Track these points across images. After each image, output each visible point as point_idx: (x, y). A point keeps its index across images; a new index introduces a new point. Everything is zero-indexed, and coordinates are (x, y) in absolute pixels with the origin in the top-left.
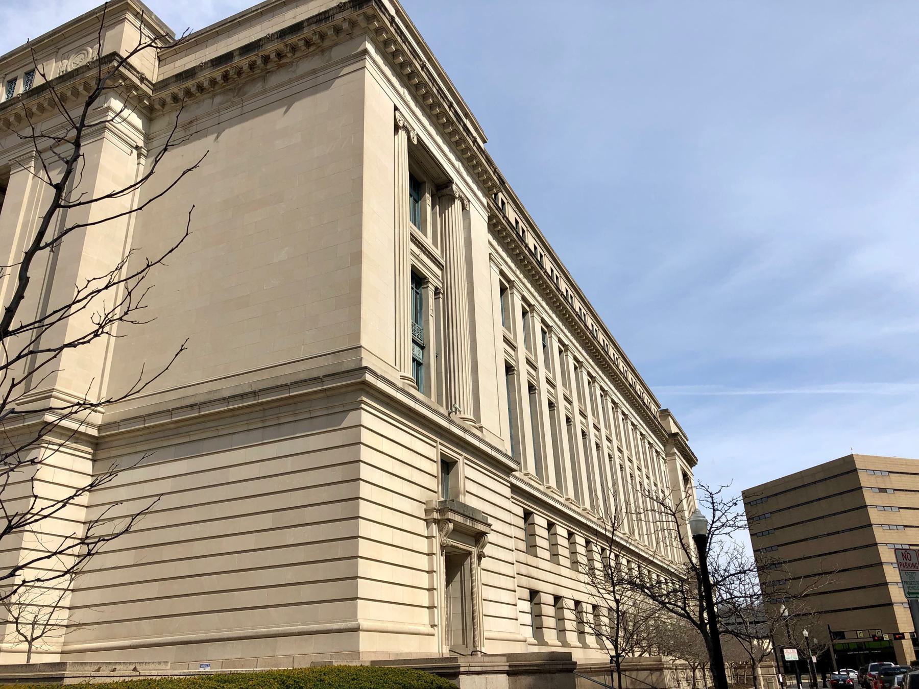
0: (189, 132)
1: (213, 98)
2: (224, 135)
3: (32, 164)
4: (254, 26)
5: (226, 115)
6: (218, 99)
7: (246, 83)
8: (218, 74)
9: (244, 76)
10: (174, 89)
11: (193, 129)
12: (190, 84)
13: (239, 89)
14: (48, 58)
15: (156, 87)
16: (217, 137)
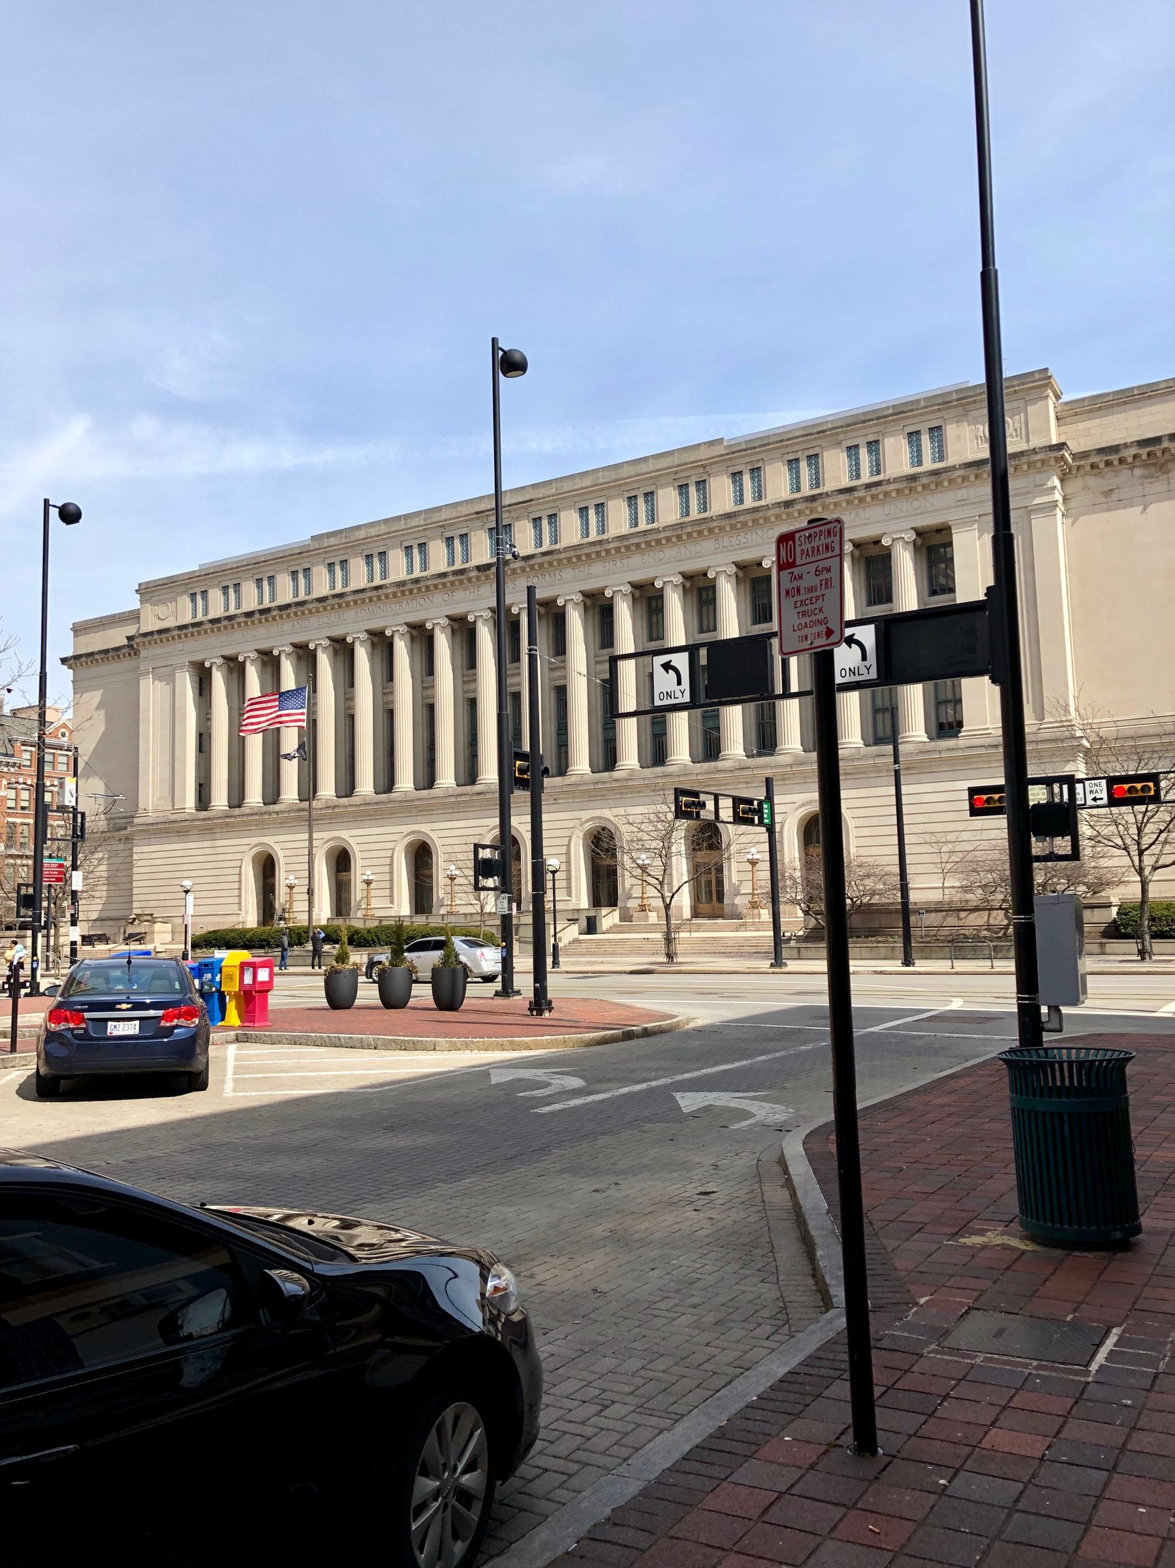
0: (1110, 499)
1: (1132, 469)
2: (1151, 508)
3: (976, 526)
4: (1168, 402)
5: (1151, 488)
6: (1138, 472)
7: (1167, 461)
8: (1144, 452)
9: (1167, 454)
10: (1095, 459)
11: (1115, 496)
12: (1114, 458)
13: (1162, 465)
15: (1075, 456)
16: (1145, 509)
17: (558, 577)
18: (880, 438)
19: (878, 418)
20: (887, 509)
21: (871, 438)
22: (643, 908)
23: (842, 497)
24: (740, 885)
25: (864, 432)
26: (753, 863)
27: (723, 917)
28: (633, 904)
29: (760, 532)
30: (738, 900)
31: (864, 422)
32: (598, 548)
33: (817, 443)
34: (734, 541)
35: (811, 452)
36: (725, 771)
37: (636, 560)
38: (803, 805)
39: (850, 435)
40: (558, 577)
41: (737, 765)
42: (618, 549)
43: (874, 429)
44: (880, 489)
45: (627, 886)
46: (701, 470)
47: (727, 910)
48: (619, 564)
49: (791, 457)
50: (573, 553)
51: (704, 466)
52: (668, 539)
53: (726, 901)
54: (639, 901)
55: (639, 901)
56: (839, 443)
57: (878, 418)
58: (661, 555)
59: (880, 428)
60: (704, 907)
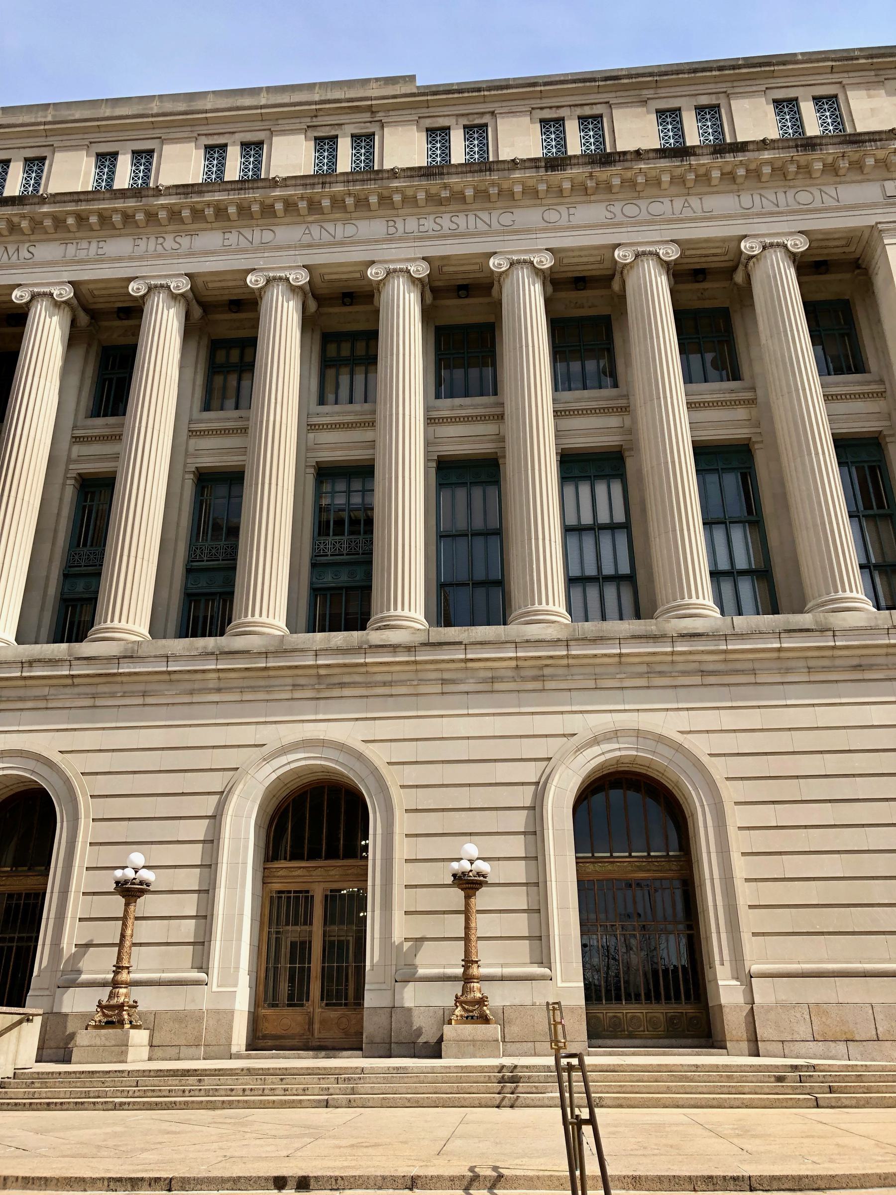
14: (869, 85)
17: (24, 253)
18: (723, 102)
19: (720, 69)
20: (746, 200)
21: (704, 100)
22: (113, 1017)
23: (664, 163)
24: (415, 951)
25: (692, 89)
26: (469, 884)
27: (353, 1043)
28: (79, 1003)
29: (485, 216)
30: (411, 996)
31: (695, 71)
32: (131, 203)
33: (604, 97)
34: (429, 224)
35: (587, 111)
36: (394, 648)
37: (211, 239)
38: (596, 741)
39: (663, 92)
40: (24, 253)
41: (422, 638)
42: (174, 214)
43: (712, 88)
44: (741, 157)
45: (68, 947)
46: (367, 116)
47: (371, 1026)
48: (169, 243)
49: (548, 114)
50: (71, 207)
51: (370, 109)
52: (290, 205)
53: (369, 1000)
54: (103, 994)
55: (103, 994)
56: (644, 102)
57: (720, 69)
58: (268, 236)
59: (721, 87)
60: (288, 1019)
